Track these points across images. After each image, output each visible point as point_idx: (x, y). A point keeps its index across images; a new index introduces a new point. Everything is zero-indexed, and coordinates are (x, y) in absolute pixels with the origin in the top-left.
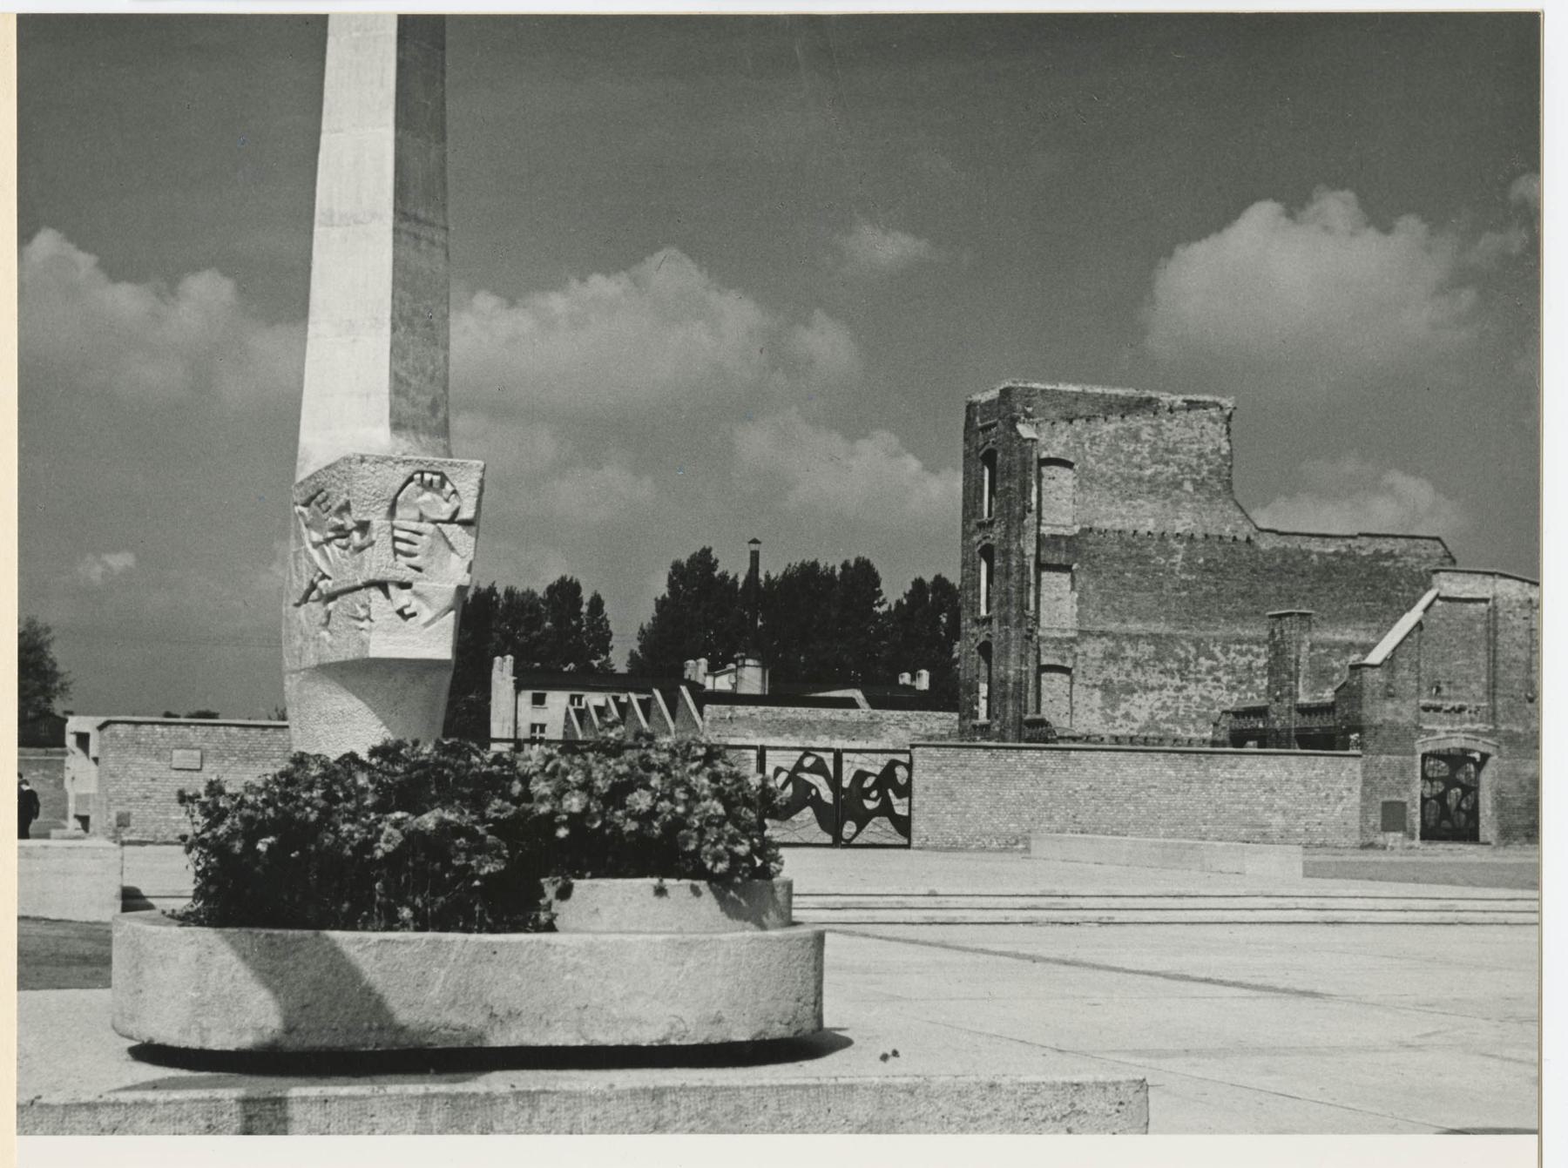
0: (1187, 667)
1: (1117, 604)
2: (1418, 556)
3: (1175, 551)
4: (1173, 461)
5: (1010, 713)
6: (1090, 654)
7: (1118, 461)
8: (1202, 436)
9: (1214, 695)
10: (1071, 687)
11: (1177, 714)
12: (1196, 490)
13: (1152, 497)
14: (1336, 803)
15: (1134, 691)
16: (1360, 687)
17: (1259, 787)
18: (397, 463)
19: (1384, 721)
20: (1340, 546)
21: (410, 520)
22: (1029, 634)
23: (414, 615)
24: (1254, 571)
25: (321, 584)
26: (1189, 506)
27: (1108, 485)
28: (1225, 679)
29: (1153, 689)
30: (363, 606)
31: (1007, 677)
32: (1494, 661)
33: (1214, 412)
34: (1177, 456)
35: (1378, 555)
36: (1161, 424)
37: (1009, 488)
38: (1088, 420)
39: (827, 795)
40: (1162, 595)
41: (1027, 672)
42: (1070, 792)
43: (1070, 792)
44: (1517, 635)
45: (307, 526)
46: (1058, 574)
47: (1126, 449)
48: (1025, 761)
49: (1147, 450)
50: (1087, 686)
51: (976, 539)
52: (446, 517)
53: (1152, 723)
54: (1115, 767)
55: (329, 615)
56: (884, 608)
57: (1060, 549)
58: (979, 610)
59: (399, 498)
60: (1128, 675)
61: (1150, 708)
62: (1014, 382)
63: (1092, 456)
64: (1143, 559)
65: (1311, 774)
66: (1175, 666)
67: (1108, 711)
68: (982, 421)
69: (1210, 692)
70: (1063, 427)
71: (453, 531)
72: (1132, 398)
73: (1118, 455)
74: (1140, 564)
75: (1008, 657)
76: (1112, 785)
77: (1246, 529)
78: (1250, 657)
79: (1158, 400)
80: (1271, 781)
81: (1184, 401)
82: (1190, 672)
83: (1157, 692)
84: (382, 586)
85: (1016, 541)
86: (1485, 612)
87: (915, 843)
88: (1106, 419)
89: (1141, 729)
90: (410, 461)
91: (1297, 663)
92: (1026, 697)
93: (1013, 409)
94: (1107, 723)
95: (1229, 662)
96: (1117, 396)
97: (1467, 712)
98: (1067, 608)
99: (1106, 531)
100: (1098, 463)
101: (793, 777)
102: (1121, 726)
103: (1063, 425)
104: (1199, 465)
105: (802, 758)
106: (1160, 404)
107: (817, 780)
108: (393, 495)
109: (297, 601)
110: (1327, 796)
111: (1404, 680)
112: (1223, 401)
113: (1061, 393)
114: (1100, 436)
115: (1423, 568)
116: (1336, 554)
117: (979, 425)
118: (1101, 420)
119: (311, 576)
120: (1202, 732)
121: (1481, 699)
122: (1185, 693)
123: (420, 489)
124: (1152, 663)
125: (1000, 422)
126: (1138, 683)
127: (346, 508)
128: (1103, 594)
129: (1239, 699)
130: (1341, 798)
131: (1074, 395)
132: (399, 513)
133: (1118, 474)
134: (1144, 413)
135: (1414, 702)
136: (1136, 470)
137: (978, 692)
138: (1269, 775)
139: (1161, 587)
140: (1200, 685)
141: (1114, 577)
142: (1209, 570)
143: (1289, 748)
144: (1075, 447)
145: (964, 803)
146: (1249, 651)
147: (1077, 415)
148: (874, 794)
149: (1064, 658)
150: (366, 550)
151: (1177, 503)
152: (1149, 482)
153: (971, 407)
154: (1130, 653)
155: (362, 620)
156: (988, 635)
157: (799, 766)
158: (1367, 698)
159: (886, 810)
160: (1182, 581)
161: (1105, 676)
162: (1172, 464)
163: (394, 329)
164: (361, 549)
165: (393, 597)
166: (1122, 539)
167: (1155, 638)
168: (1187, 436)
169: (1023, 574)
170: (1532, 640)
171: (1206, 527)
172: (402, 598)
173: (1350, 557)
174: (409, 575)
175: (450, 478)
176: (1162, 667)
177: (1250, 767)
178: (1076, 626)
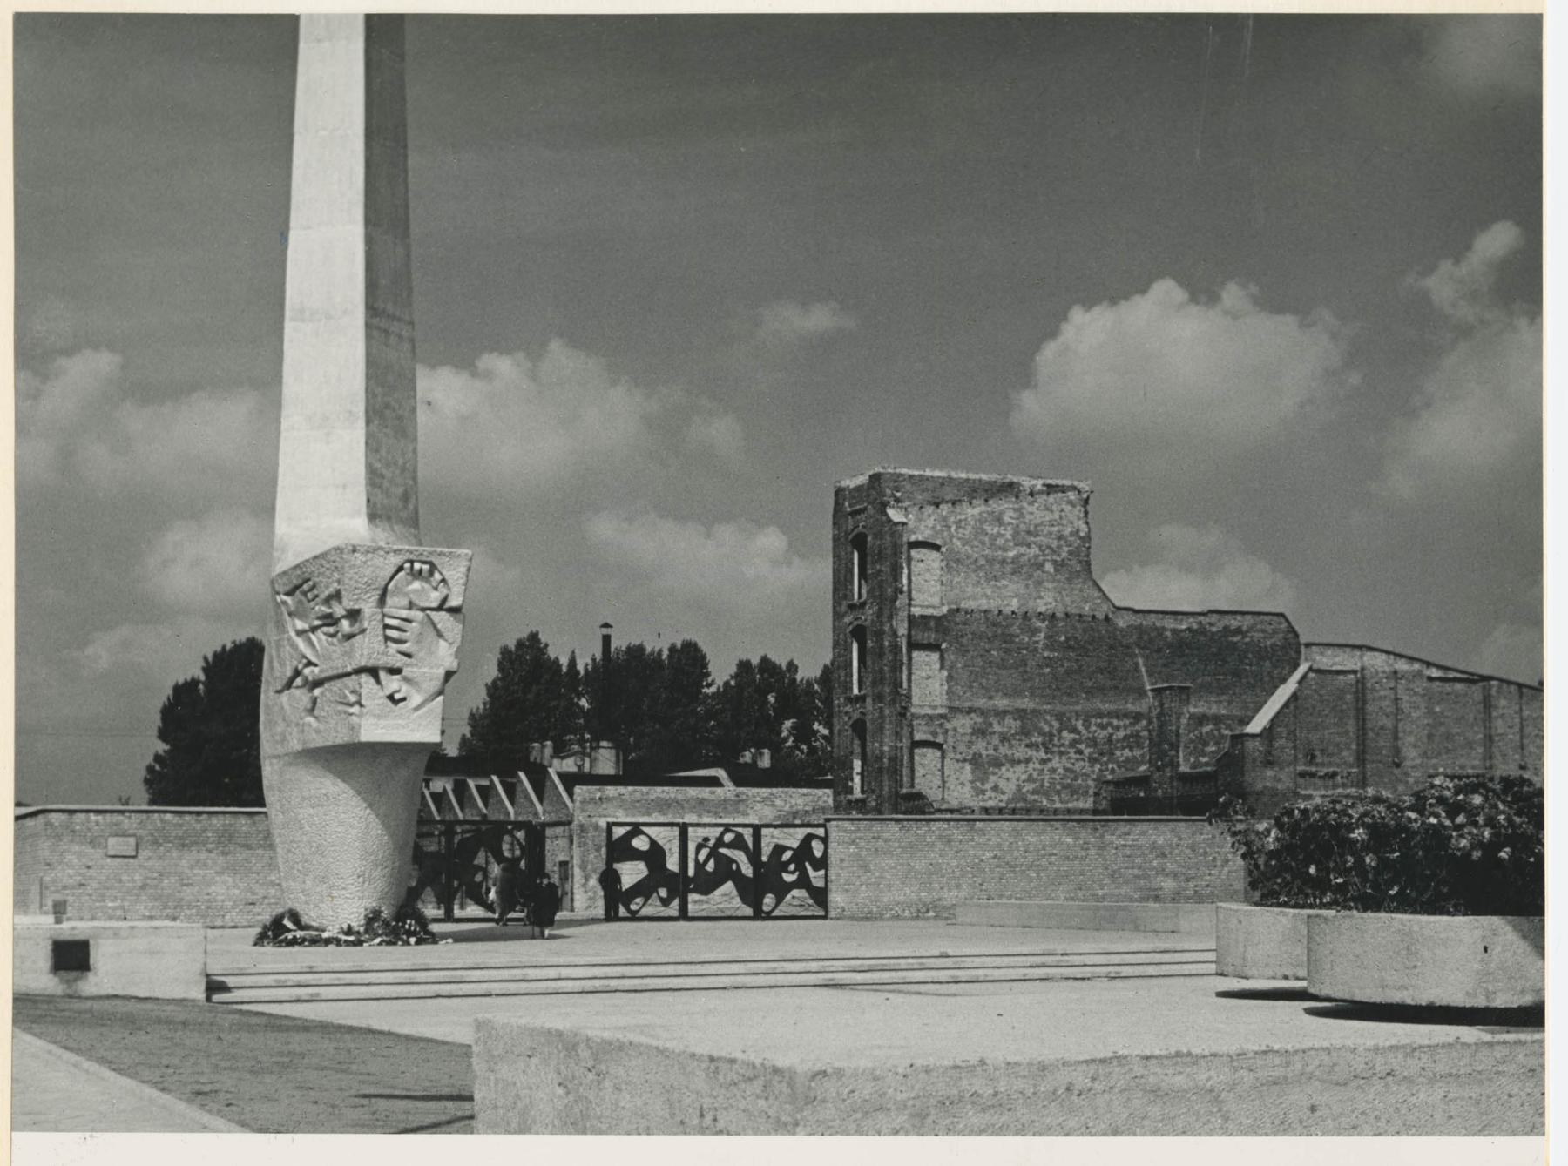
0: (1051, 741)
1: (984, 681)
2: (1263, 631)
3: (1038, 630)
4: (1035, 543)
5: (886, 789)
6: (960, 730)
7: (983, 543)
8: (1061, 518)
9: (1077, 767)
10: (943, 762)
11: (1042, 786)
12: (1056, 570)
14: (1223, 866)
15: (1003, 765)
16: (1242, 756)
17: (1151, 851)
18: (388, 553)
19: (1265, 787)
21: (400, 608)
23: (403, 699)
24: (1112, 647)
25: (307, 671)
26: (1050, 586)
27: (973, 566)
28: (1087, 751)
29: (1019, 762)
30: (353, 692)
31: (882, 753)
32: (1363, 729)
33: (1072, 496)
34: (1038, 539)
35: (1227, 631)
36: (1022, 508)
37: (880, 571)
38: (953, 504)
39: (747, 870)
40: (1026, 672)
41: (901, 748)
42: (977, 861)
43: (977, 861)
44: (1385, 703)
45: (290, 614)
46: (929, 653)
47: (990, 532)
48: (933, 832)
50: (958, 761)
51: (847, 620)
52: (435, 605)
53: (1019, 796)
54: (1018, 834)
55: (314, 701)
56: (713, 689)
57: (930, 629)
58: (851, 689)
59: (390, 587)
60: (996, 749)
61: (1018, 780)
62: (883, 468)
63: (959, 539)
64: (1008, 638)
65: (1199, 838)
66: (1040, 740)
67: (979, 784)
68: (850, 506)
69: (1073, 764)
70: (930, 511)
71: (441, 618)
72: (995, 482)
73: (982, 538)
74: (1005, 642)
75: (882, 734)
76: (1016, 854)
77: (1105, 608)
78: (1110, 730)
79: (1019, 484)
80: (1161, 846)
82: (1054, 745)
83: (1023, 765)
84: (373, 672)
86: (1353, 682)
87: (832, 914)
88: (971, 503)
89: (1008, 802)
90: (400, 550)
91: (1178, 735)
92: (901, 771)
94: (977, 795)
95: (1091, 735)
96: (980, 480)
97: (1339, 777)
98: (937, 686)
100: (964, 545)
101: (714, 853)
102: (990, 798)
103: (930, 509)
104: (1059, 547)
105: (722, 834)
107: (740, 857)
108: (383, 583)
109: (279, 688)
110: (1215, 858)
111: (1282, 748)
112: (1081, 485)
113: (928, 479)
114: (966, 519)
115: (1269, 643)
116: (1189, 629)
117: (849, 509)
118: (965, 505)
119: (295, 663)
120: (1067, 802)
121: (1351, 766)
122: (1050, 765)
123: (410, 578)
124: (1018, 737)
125: (870, 507)
126: (1006, 755)
127: (337, 596)
128: (971, 672)
129: (1101, 770)
130: (1227, 861)
132: (389, 601)
134: (1006, 497)
135: (1291, 769)
136: (1000, 553)
137: (852, 768)
138: (1160, 841)
139: (1026, 665)
140: (1063, 758)
141: (981, 656)
142: (1070, 647)
143: (1172, 815)
144: (942, 531)
145: (877, 874)
146: (1110, 724)
147: (943, 499)
148: (792, 867)
149: (935, 734)
150: (358, 637)
151: (1039, 583)
152: (1013, 562)
153: (839, 492)
154: (997, 728)
155: (351, 705)
156: (861, 713)
157: (720, 842)
158: (1248, 766)
159: (803, 882)
160: (1045, 658)
163: (368, 422)
164: (350, 637)
165: (384, 683)
166: (987, 619)
167: (1020, 714)
168: (1047, 519)
169: (896, 654)
170: (1397, 709)
171: (1066, 607)
172: (392, 684)
173: (1202, 633)
174: (398, 661)
175: (439, 567)
176: (1028, 741)
177: (1143, 833)
178: (946, 703)
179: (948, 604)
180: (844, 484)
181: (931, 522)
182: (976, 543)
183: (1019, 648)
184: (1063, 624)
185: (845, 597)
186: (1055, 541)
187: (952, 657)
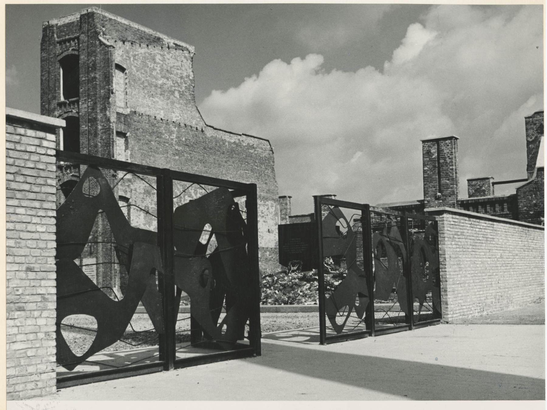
2: (262, 149)
5: (101, 226)
6: (138, 190)
12: (180, 97)
13: (161, 97)
20: (236, 139)
22: (115, 174)
24: (205, 148)
26: (178, 106)
34: (172, 76)
36: (165, 55)
37: (95, 78)
38: (132, 44)
40: (168, 157)
47: (150, 66)
49: (159, 69)
63: (135, 67)
64: (159, 135)
72: (152, 35)
73: (146, 69)
81: (174, 44)
85: (101, 112)
93: (95, 27)
96: (145, 32)
99: (142, 114)
100: (137, 71)
103: (120, 43)
104: (181, 83)
106: (164, 43)
113: (119, 23)
114: (138, 54)
115: (263, 155)
131: (125, 26)
133: (146, 80)
136: (154, 80)
139: (167, 153)
142: (187, 145)
151: (173, 103)
152: (160, 88)
161: (145, 204)
162: (170, 80)
168: (176, 65)
169: (110, 134)
179: (131, 108)
180: (54, 22)
181: (120, 52)
182: (143, 71)
183: (164, 142)
184: (184, 130)
185: (54, 98)
186: (180, 79)
187: (132, 142)
